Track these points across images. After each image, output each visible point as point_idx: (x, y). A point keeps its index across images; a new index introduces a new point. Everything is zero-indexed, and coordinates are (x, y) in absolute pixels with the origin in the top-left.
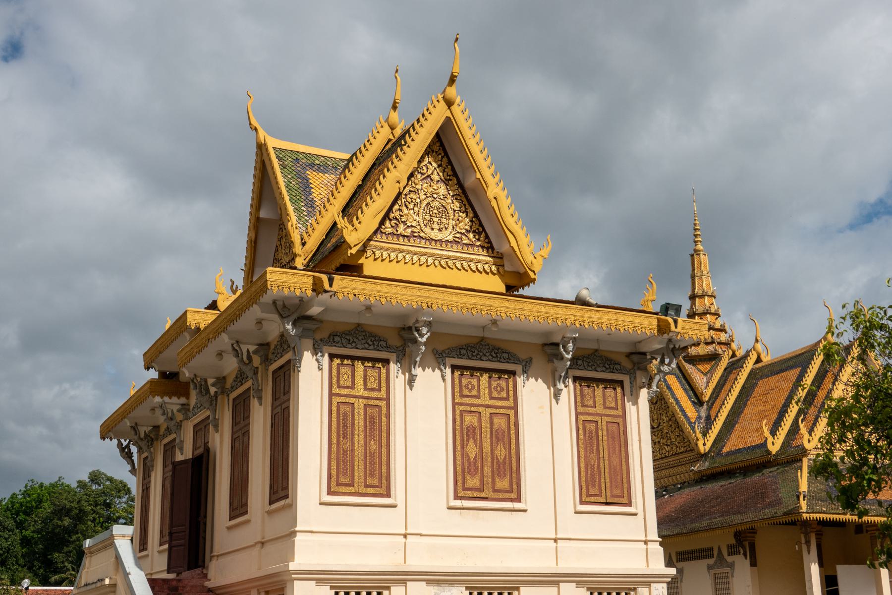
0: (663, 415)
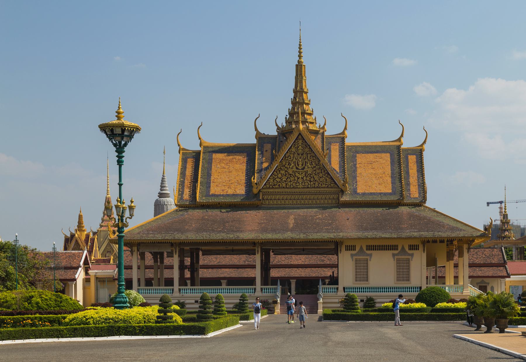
0: (307, 163)
